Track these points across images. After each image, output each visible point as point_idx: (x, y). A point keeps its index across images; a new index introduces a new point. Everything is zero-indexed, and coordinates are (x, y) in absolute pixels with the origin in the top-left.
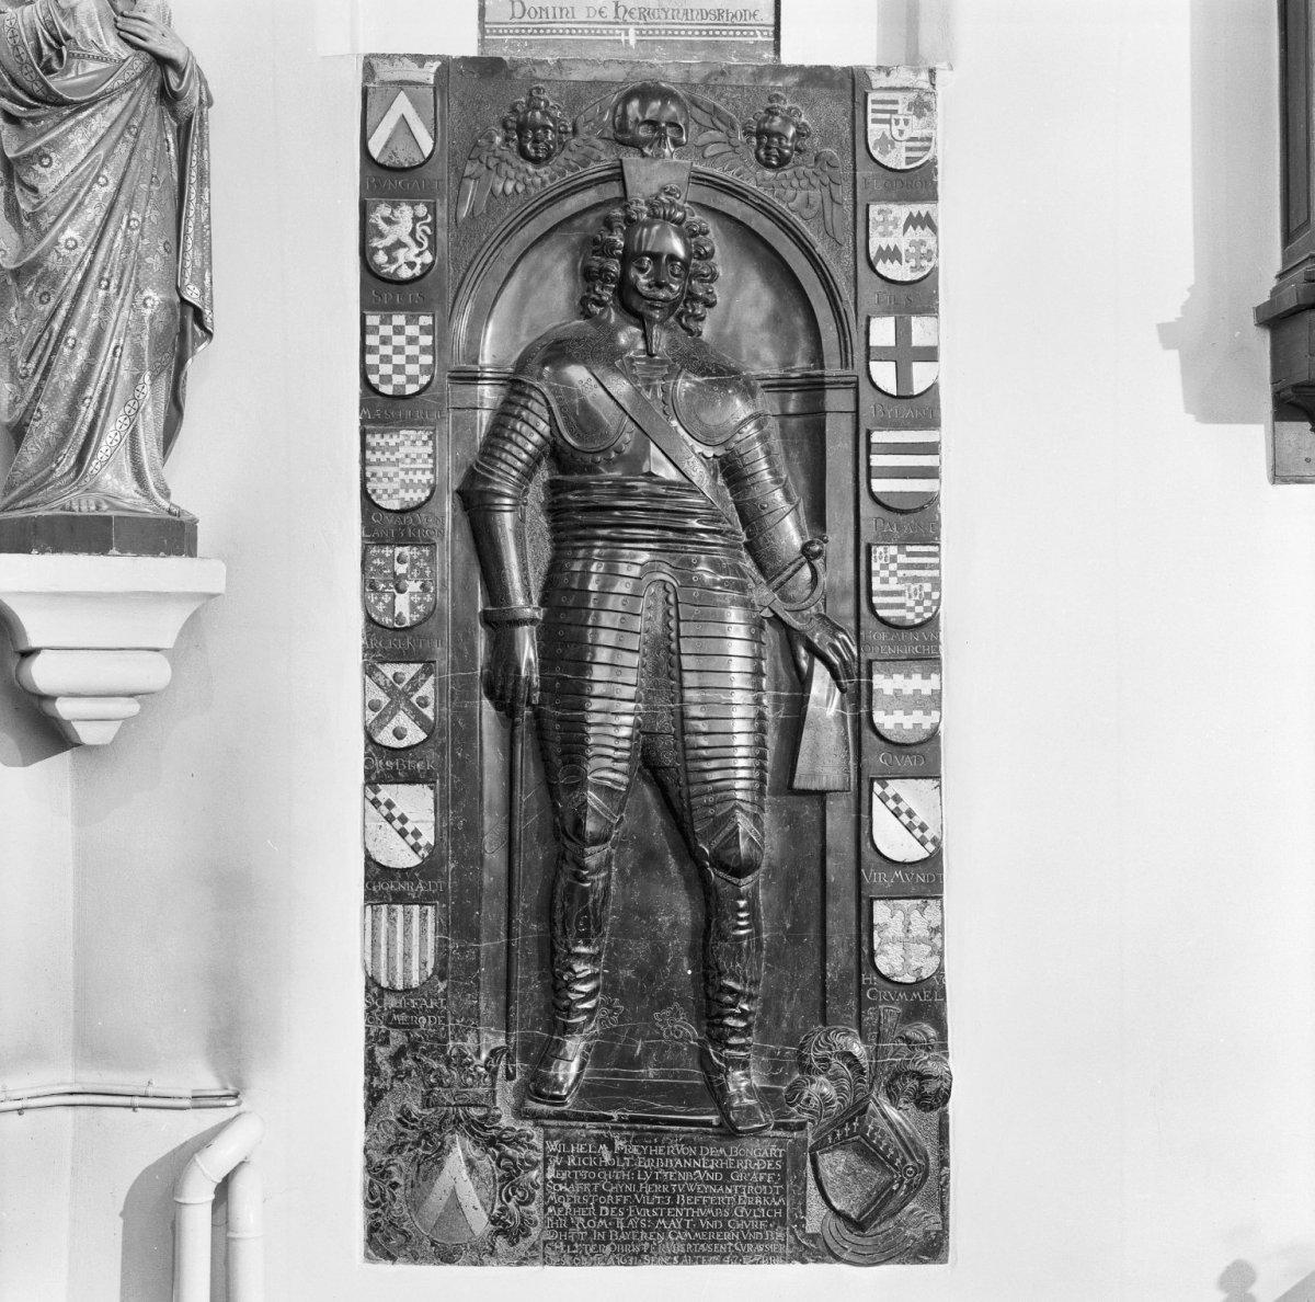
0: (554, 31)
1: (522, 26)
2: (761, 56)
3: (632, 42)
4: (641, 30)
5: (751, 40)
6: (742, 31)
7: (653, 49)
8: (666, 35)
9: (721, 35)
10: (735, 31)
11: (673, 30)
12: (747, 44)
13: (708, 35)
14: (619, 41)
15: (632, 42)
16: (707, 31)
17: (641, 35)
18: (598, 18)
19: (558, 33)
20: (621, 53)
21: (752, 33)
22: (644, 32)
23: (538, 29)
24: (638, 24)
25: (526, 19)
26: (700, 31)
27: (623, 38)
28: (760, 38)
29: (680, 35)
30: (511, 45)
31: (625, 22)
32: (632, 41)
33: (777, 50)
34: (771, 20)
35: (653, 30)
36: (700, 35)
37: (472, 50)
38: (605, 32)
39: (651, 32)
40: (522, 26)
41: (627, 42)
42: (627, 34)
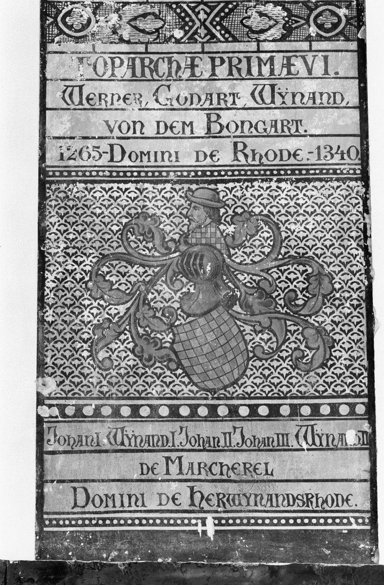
0: (122, 522)
1: (87, 516)
2: (356, 546)
3: (211, 533)
4: (220, 519)
5: (344, 529)
6: (334, 518)
7: (233, 541)
8: (248, 524)
9: (310, 524)
10: (326, 519)
11: (256, 519)
12: (340, 533)
13: (295, 524)
14: (195, 532)
15: (211, 533)
16: (295, 519)
17: (220, 524)
18: (171, 506)
19: (126, 524)
20: (201, 546)
21: (345, 521)
22: (223, 522)
23: (104, 520)
24: (217, 512)
25: (90, 508)
26: (287, 519)
27: (200, 528)
28: (354, 526)
29: (263, 524)
30: (74, 537)
31: (202, 511)
32: (211, 530)
33: (375, 539)
34: (367, 506)
35: (234, 519)
36: (287, 524)
37: (29, 554)
38: (179, 522)
39: (231, 521)
40: (87, 516)
41: (204, 532)
42: (204, 524)
